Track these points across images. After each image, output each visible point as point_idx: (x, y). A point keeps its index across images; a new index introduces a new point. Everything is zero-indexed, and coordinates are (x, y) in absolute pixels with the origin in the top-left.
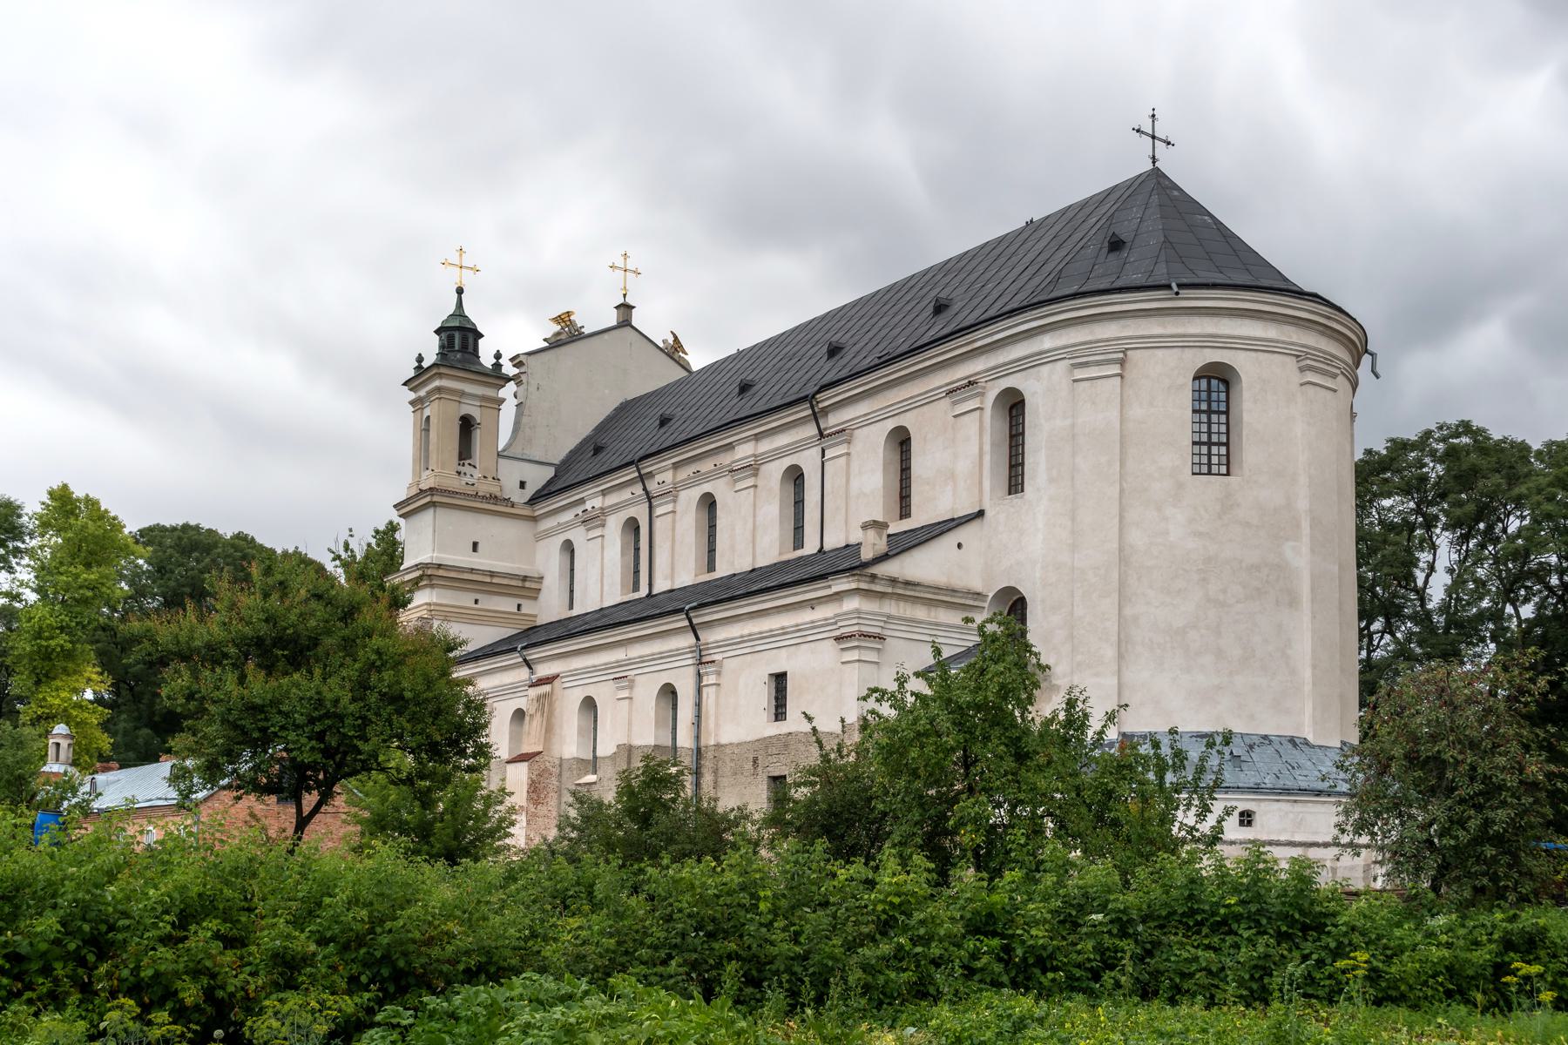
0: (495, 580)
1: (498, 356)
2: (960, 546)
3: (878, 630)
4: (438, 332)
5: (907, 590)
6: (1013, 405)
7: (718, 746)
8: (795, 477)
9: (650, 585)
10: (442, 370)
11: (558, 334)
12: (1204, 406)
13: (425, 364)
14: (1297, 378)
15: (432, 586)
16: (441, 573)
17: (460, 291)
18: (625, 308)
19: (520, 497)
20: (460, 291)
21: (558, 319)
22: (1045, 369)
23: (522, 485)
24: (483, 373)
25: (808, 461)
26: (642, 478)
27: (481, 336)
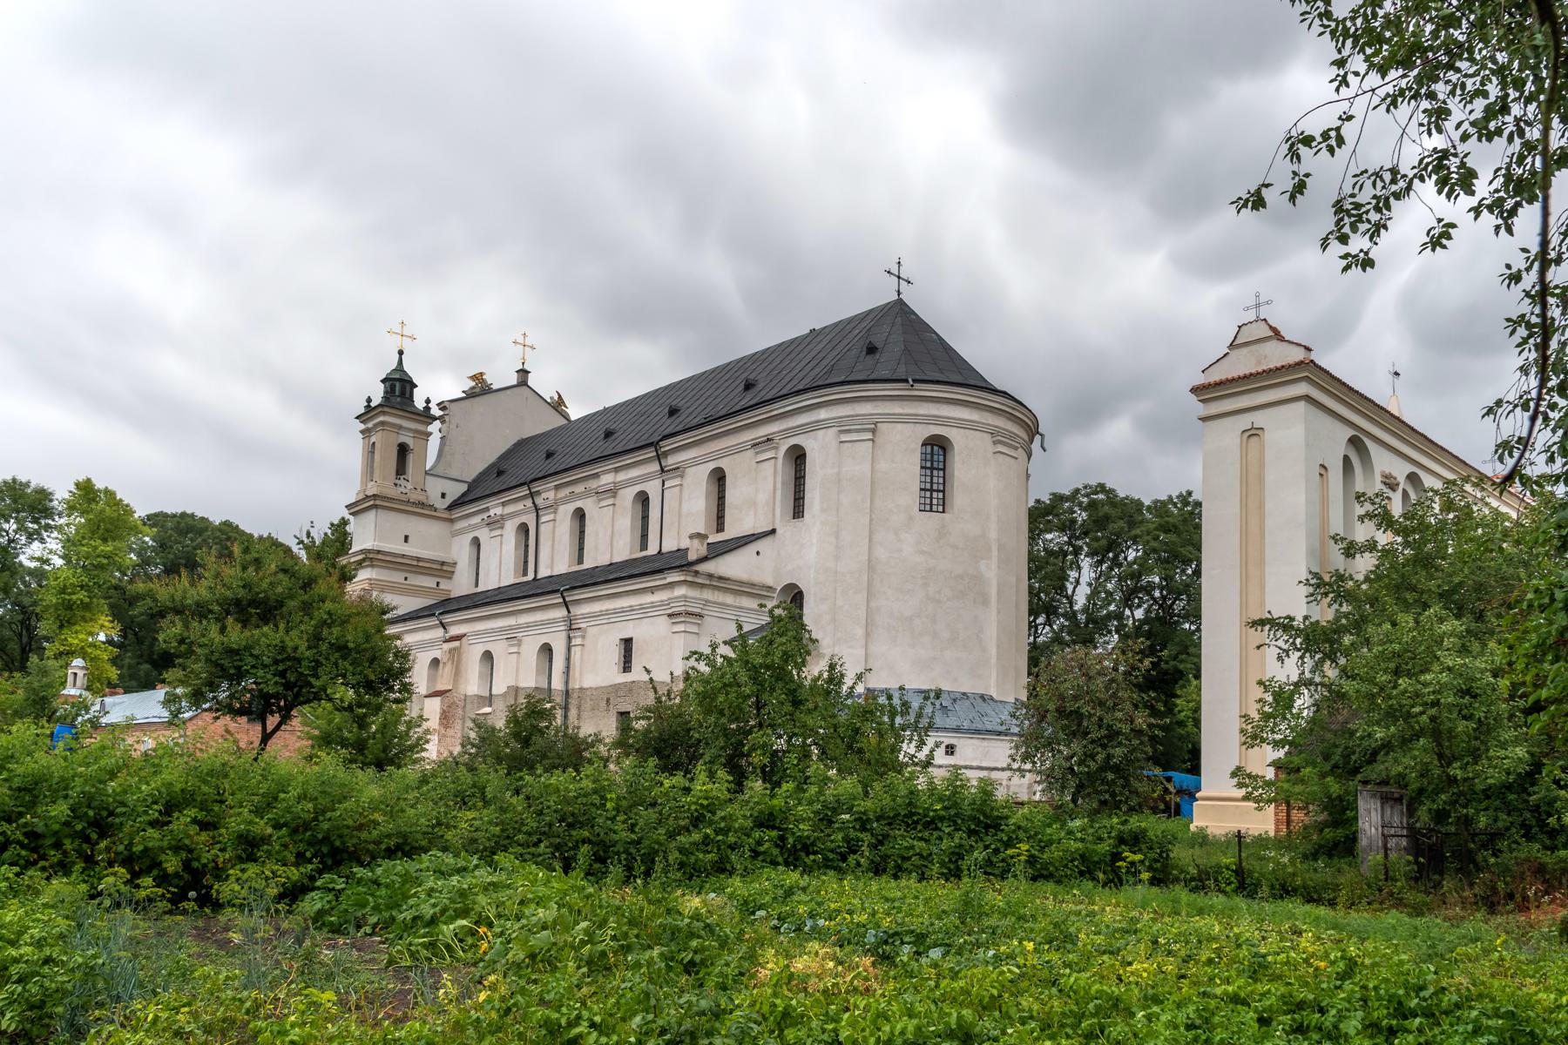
0: (421, 564)
1: (428, 401)
2: (758, 553)
3: (699, 610)
4: (383, 381)
5: (720, 583)
6: (798, 457)
7: (581, 689)
8: (643, 499)
9: (536, 572)
10: (386, 409)
11: (473, 388)
12: (929, 465)
13: (373, 404)
15: (372, 566)
16: (380, 557)
17: (401, 353)
18: (523, 373)
19: (442, 504)
20: (401, 353)
21: (473, 378)
22: (821, 433)
23: (443, 496)
24: (417, 413)
25: (653, 488)
26: (532, 495)
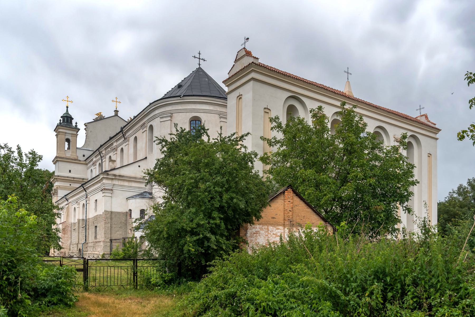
0: (75, 180)
2: (139, 166)
3: (111, 188)
5: (121, 178)
7: (89, 219)
10: (60, 127)
11: (97, 118)
14: (219, 120)
15: (58, 181)
16: (59, 178)
18: (116, 111)
19: (82, 159)
21: (97, 114)
22: (156, 119)
26: (100, 153)
27: (73, 119)
